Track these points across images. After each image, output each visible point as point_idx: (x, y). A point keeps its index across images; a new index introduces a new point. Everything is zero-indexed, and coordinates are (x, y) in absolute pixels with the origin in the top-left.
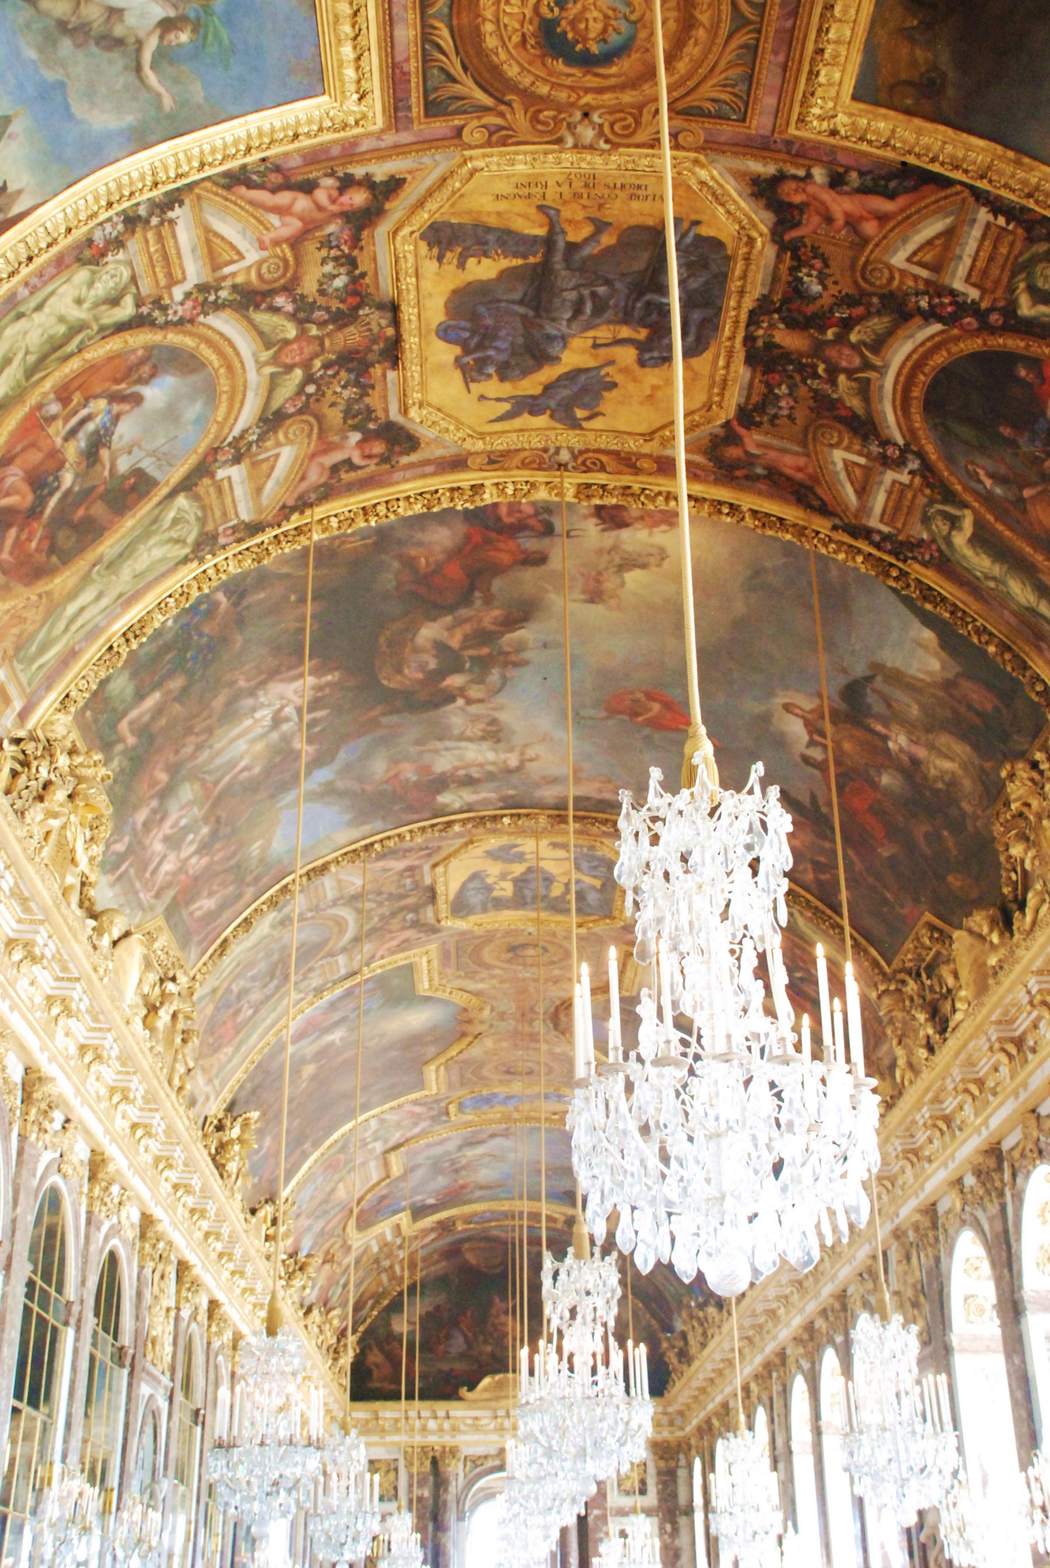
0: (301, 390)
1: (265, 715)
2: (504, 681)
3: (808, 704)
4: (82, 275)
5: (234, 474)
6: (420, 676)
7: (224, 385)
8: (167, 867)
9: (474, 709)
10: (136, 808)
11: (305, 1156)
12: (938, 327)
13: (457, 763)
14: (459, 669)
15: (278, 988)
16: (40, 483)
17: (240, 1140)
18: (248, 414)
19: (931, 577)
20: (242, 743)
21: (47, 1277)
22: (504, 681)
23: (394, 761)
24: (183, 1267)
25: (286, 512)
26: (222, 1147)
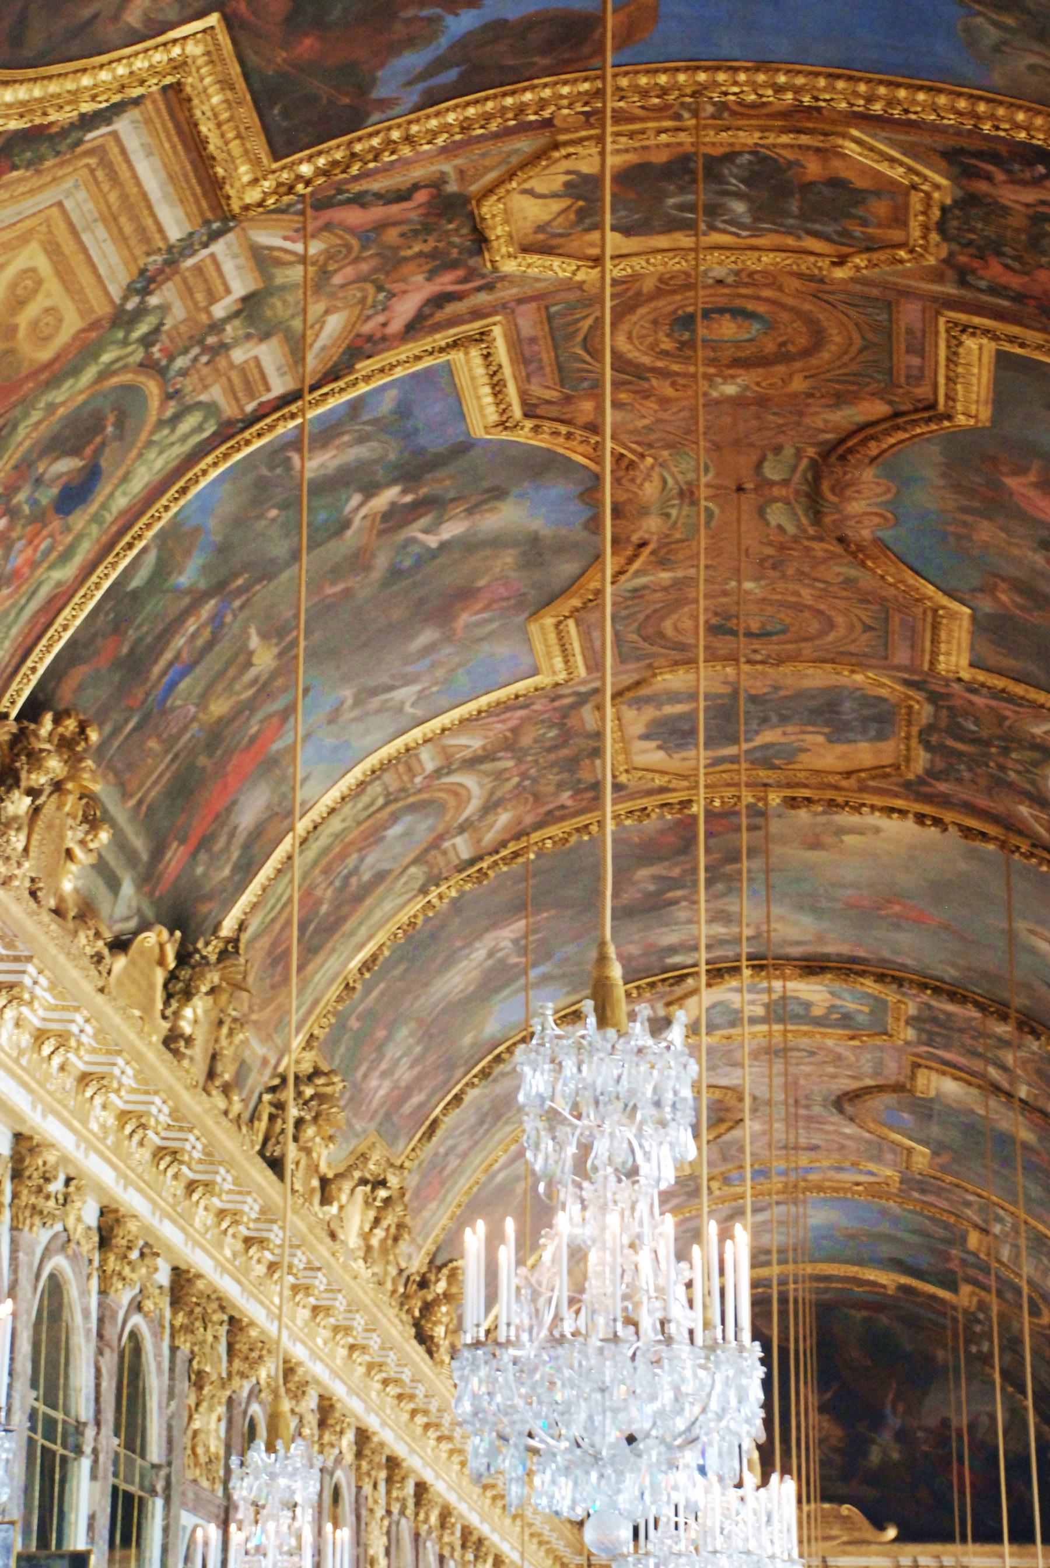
0: (519, 785)
5: (459, 841)
8: (382, 1092)
15: (487, 1131)
24: (393, 1463)
25: (504, 844)
26: (427, 1308)
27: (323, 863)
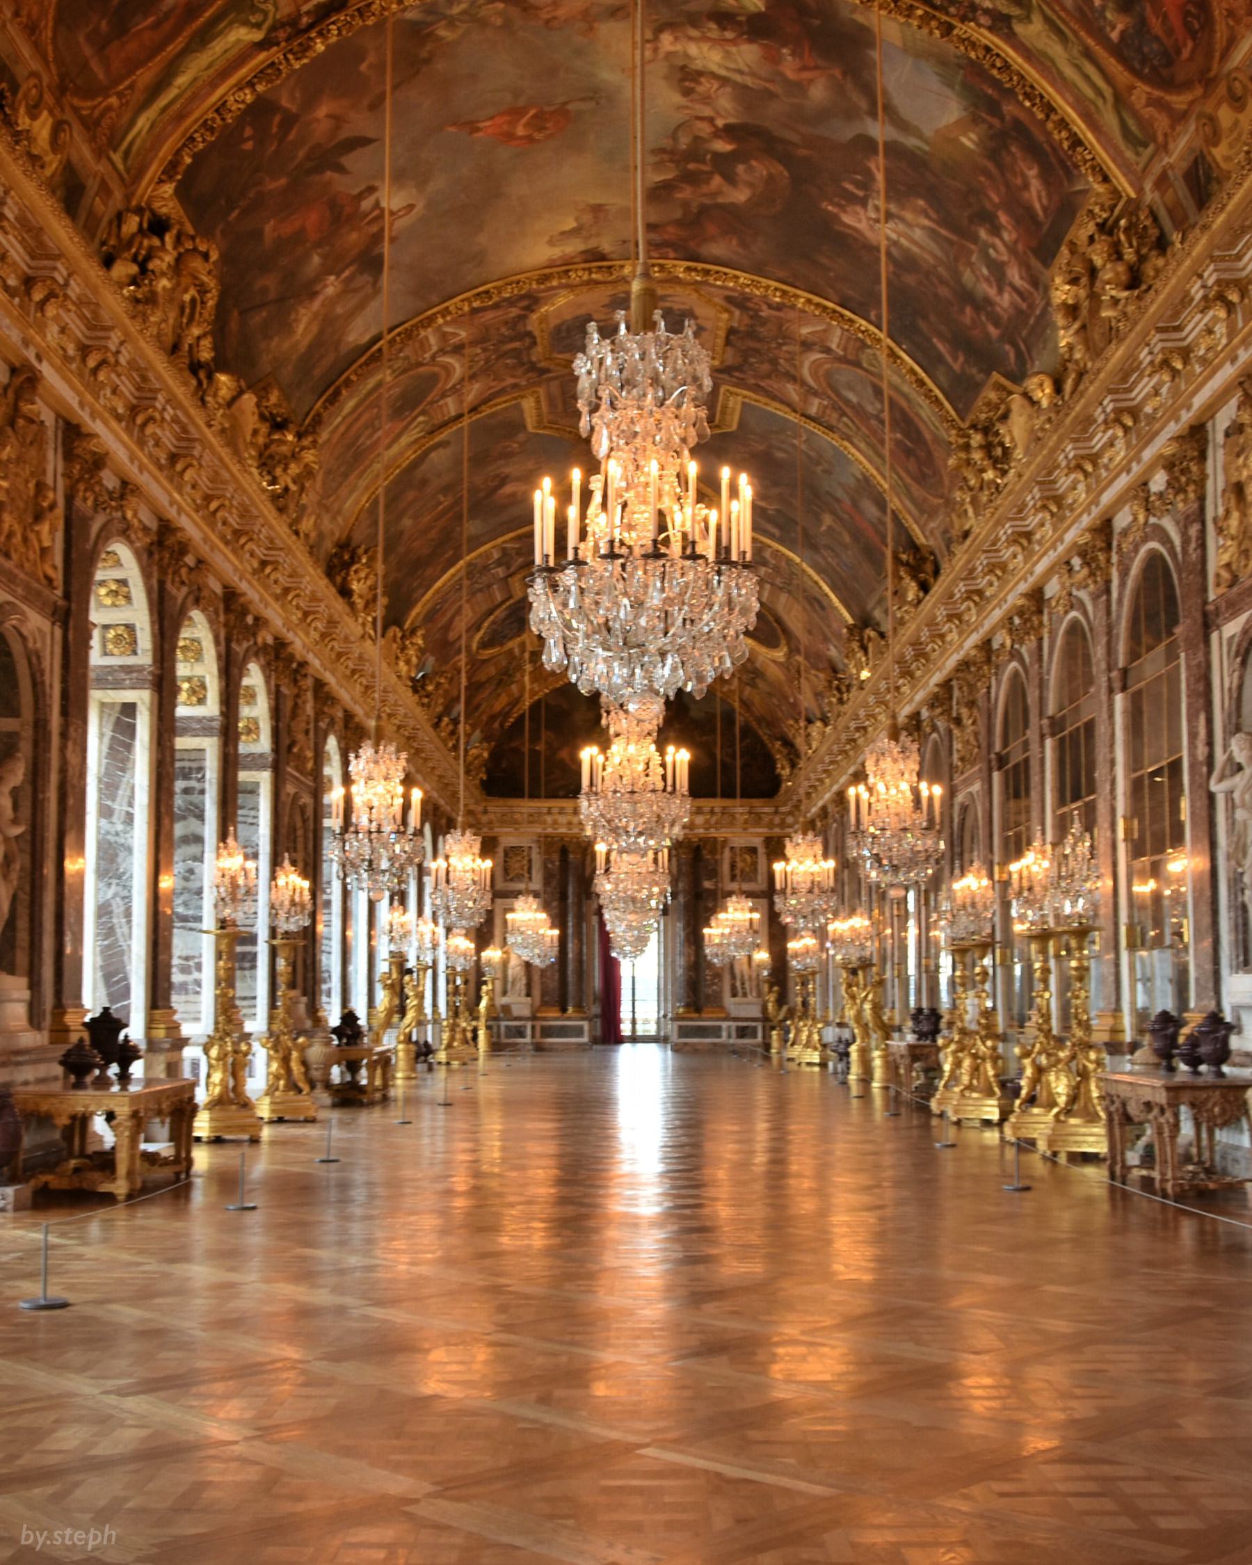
2: (674, 136)
5: (834, 346)
6: (754, 163)
9: (707, 112)
13: (734, 49)
14: (717, 156)
22: (674, 136)
23: (799, 88)
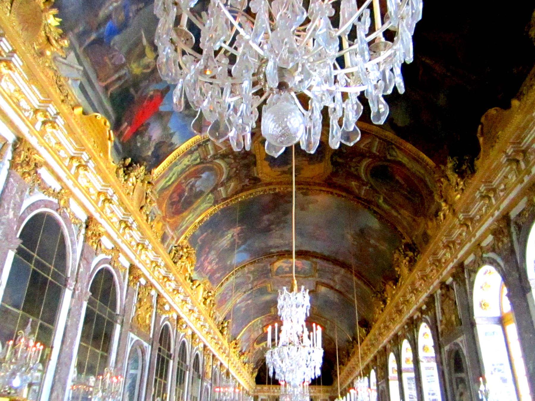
0: (235, 171)
1: (230, 235)
3: (353, 232)
4: (189, 156)
5: (222, 189)
7: (219, 172)
8: (209, 268)
10: (201, 257)
11: (243, 328)
12: (370, 160)
14: (273, 224)
16: (180, 196)
17: (227, 326)
18: (224, 177)
19: (375, 209)
20: (225, 241)
21: (182, 361)
24: (214, 356)
25: (233, 195)
26: (223, 328)
27: (184, 175)
